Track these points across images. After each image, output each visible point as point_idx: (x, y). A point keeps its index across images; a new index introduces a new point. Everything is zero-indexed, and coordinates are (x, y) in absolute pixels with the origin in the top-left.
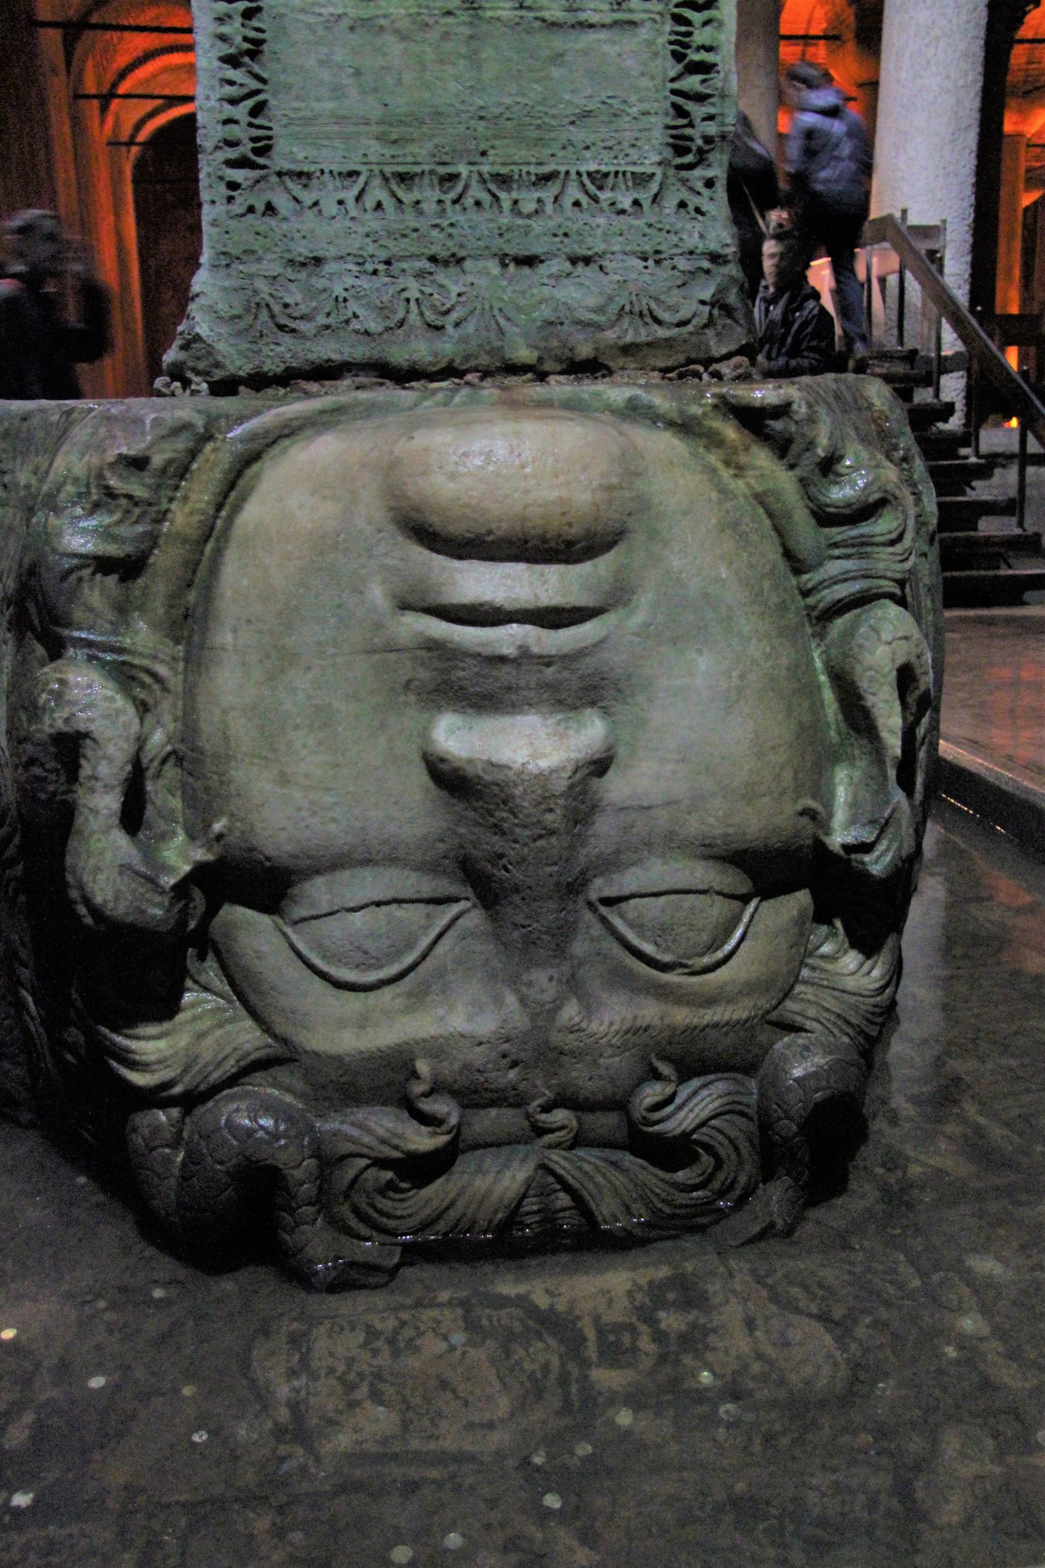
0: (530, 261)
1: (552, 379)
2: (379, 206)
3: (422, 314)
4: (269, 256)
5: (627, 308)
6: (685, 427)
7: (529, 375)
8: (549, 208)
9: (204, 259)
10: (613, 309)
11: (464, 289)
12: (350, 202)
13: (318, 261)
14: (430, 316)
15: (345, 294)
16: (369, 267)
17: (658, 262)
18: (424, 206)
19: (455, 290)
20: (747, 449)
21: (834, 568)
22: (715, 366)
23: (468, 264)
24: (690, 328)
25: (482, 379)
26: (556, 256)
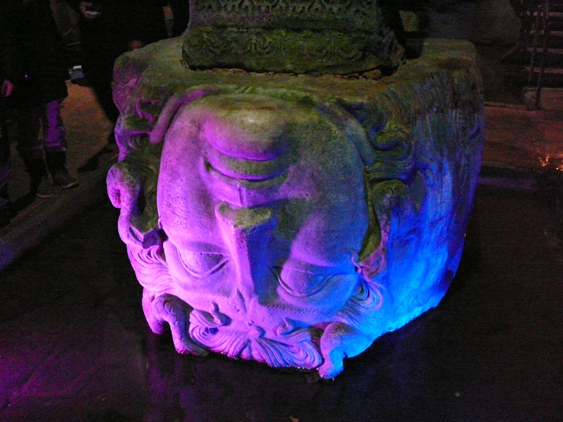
0: (299, 30)
1: (299, 75)
2: (247, 7)
3: (256, 48)
4: (209, 24)
5: (330, 51)
7: (291, 74)
8: (306, 11)
9: (189, 24)
10: (324, 51)
11: (272, 40)
12: (237, 5)
13: (225, 27)
14: (259, 49)
16: (241, 30)
17: (345, 33)
18: (262, 8)
19: (269, 40)
20: (346, 119)
21: (377, 165)
22: (366, 74)
23: (275, 31)
24: (353, 60)
25: (275, 74)
26: (307, 29)
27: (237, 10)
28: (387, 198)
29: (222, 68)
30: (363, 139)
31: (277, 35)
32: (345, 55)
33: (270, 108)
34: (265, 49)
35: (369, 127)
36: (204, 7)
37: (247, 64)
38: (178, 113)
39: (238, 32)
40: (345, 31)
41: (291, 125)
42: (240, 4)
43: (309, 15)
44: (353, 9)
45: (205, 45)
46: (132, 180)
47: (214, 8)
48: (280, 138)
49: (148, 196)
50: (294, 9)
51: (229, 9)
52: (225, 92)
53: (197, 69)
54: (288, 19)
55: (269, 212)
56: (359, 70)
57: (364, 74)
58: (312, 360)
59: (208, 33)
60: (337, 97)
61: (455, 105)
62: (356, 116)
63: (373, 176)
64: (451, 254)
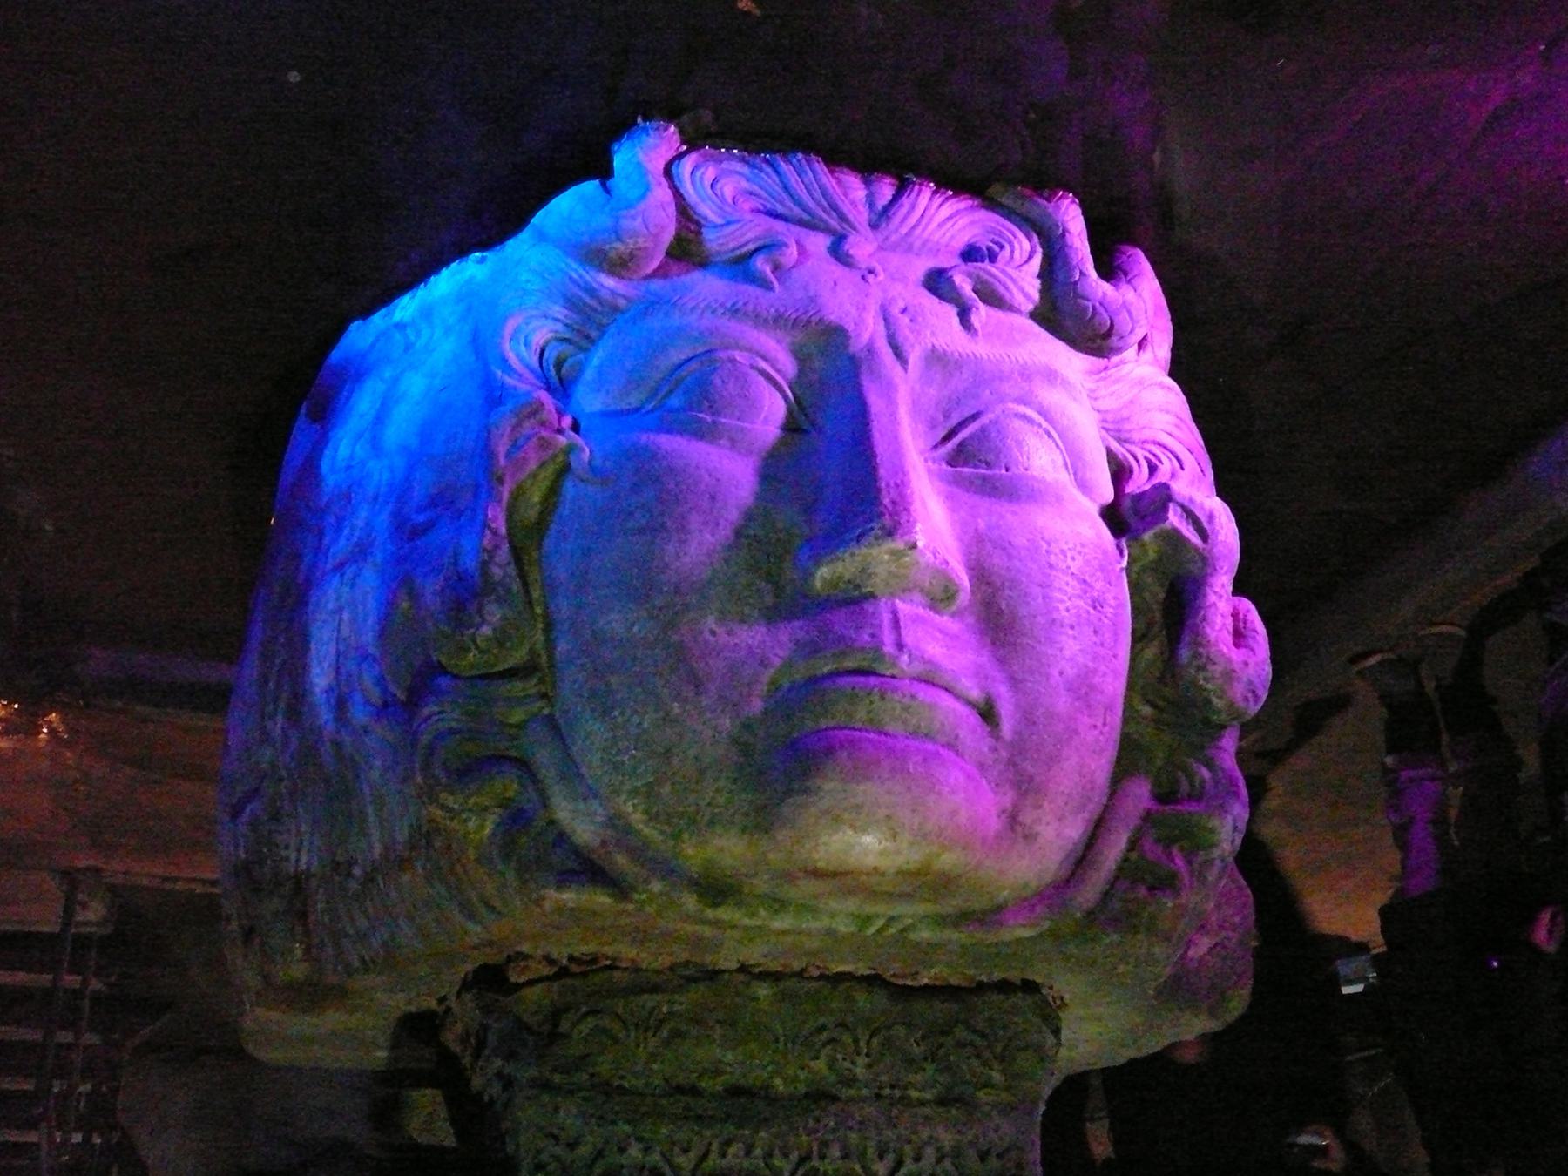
0: (735, 1091)
1: (735, 966)
2: (881, 1157)
3: (856, 1041)
4: (987, 1108)
5: (650, 1034)
6: (667, 869)
7: (757, 970)
8: (715, 1147)
9: (1042, 1108)
10: (665, 1033)
11: (812, 1064)
12: (908, 1161)
13: (942, 1102)
14: (847, 1038)
15: (926, 1065)
17: (608, 1084)
18: (838, 1154)
19: (820, 1065)
20: (604, 843)
21: (517, 716)
22: (547, 971)
23: (802, 1089)
24: (584, 1009)
25: (803, 970)
26: (713, 1095)
27: (907, 1148)
28: (489, 624)
29: (951, 986)
30: (556, 788)
31: (795, 1079)
32: (606, 1022)
33: (817, 874)
34: (832, 1041)
35: (540, 823)
36: (999, 1156)
37: (881, 999)
38: (1072, 860)
39: (906, 1088)
40: (607, 1089)
41: (757, 827)
42: (899, 1164)
43: (708, 1133)
44: (584, 1151)
45: (998, 1050)
46: (1201, 675)
47: (972, 1154)
48: (789, 792)
49: (1156, 629)
50: (748, 1153)
51: (930, 1152)
52: (942, 921)
53: (1018, 982)
54: (765, 1122)
55: (818, 584)
56: (569, 981)
57: (555, 969)
58: (698, 174)
59: (988, 1084)
60: (630, 907)
61: (299, 883)
62: (577, 852)
63: (530, 686)
64: (311, 468)
